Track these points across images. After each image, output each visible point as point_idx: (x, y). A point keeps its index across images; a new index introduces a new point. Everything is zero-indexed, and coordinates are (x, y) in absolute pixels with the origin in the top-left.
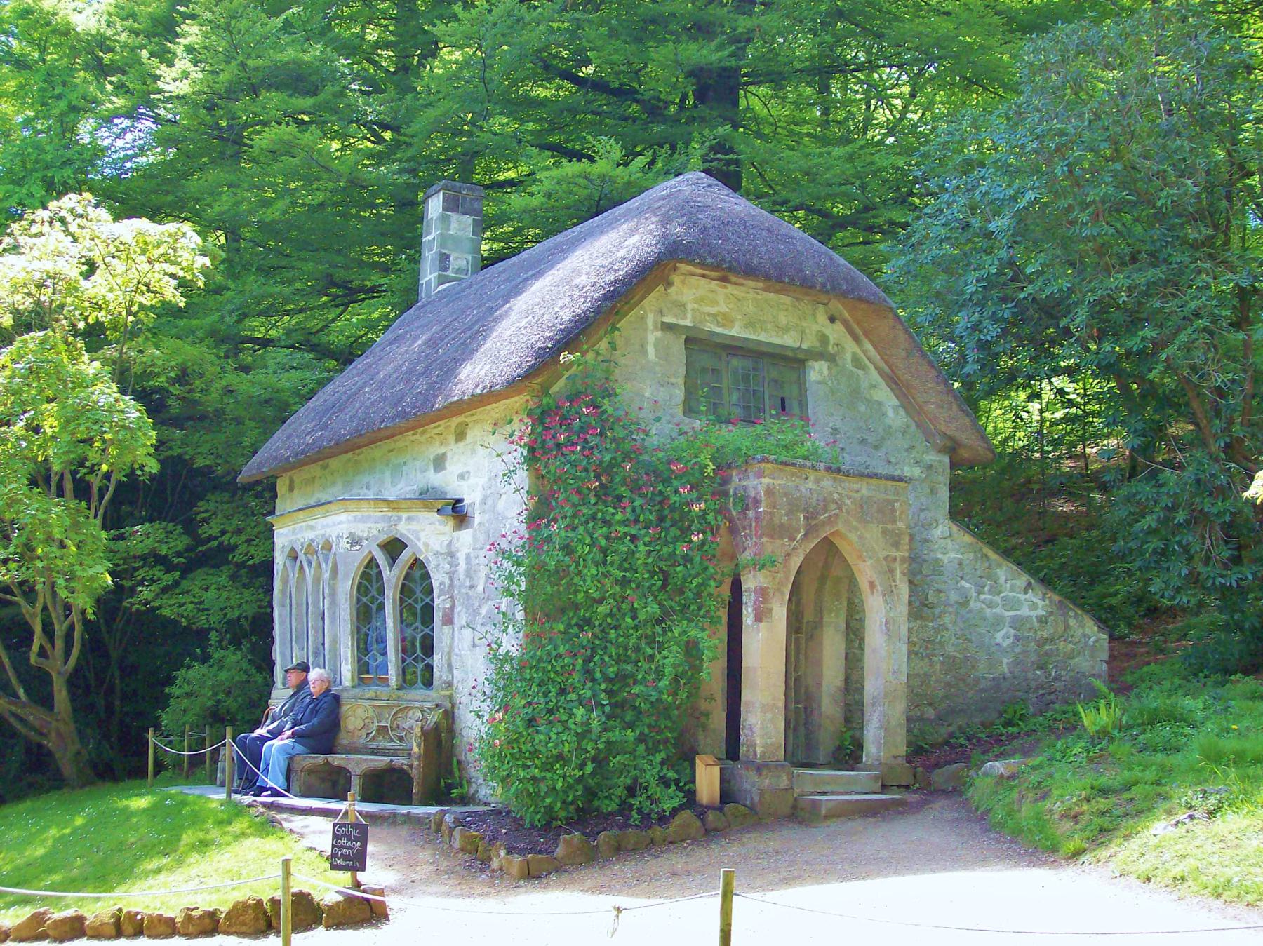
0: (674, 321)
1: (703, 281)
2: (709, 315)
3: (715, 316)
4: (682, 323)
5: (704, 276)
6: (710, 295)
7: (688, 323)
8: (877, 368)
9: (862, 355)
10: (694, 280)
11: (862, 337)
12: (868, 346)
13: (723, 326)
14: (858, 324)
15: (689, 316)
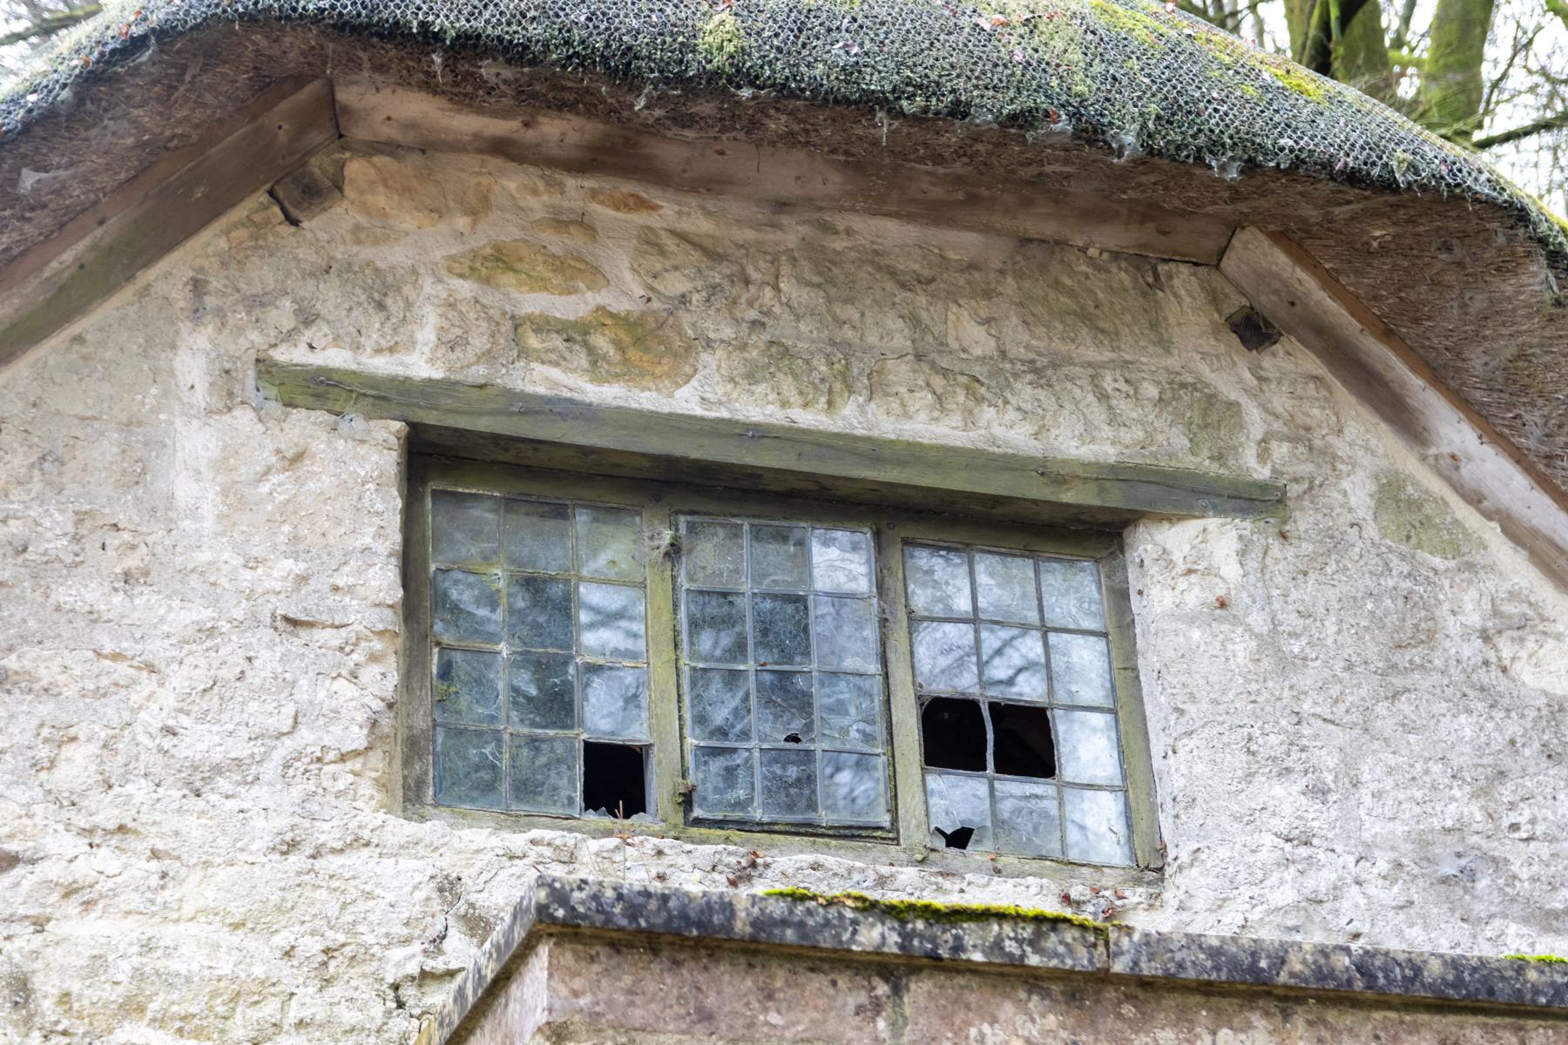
0: (336, 358)
1: (512, 182)
2: (543, 325)
3: (575, 333)
4: (382, 365)
5: (501, 148)
6: (556, 242)
7: (420, 365)
8: (1515, 531)
9: (1437, 486)
10: (467, 173)
11: (1416, 387)
12: (1455, 432)
13: (627, 373)
14: (1388, 335)
15: (427, 334)
